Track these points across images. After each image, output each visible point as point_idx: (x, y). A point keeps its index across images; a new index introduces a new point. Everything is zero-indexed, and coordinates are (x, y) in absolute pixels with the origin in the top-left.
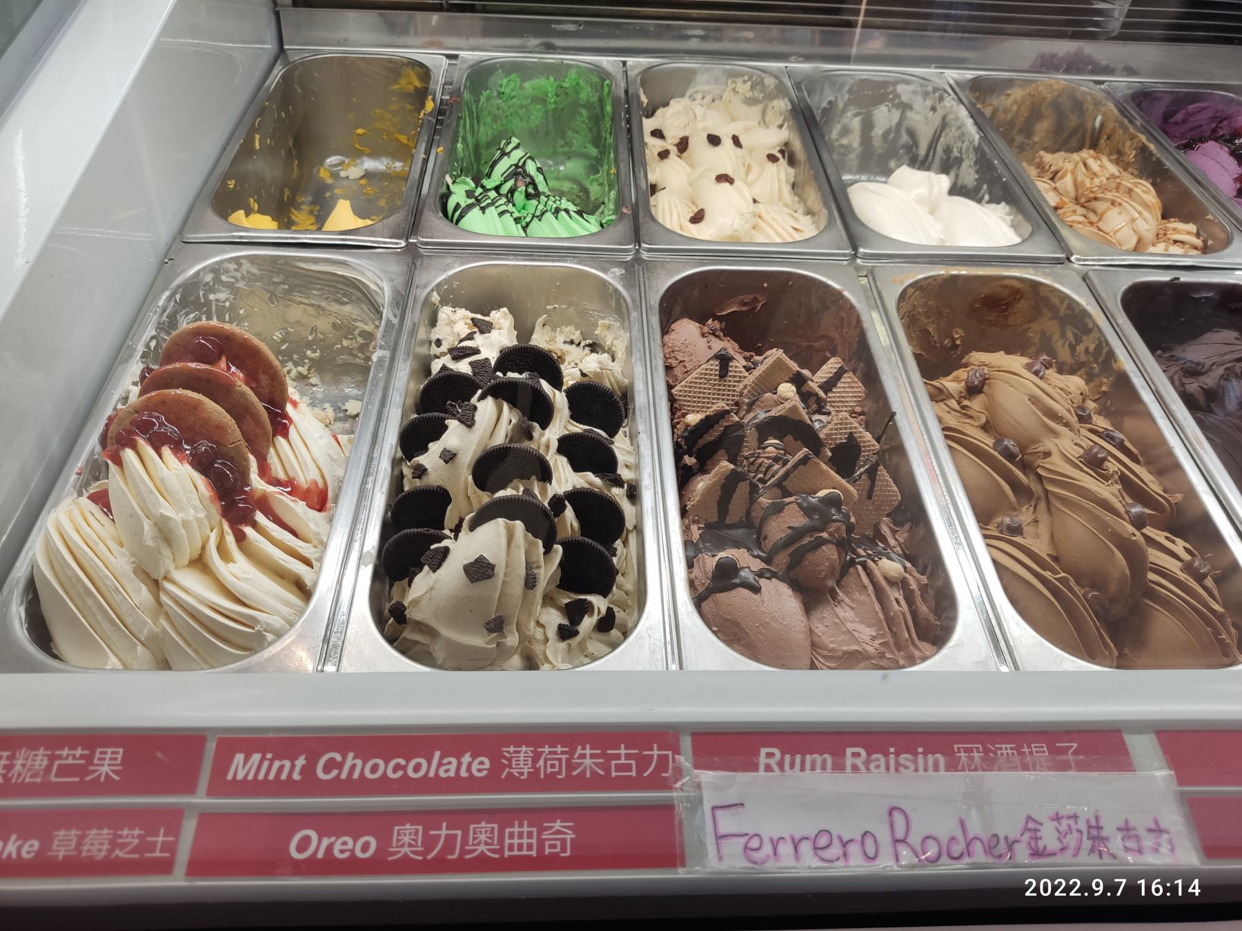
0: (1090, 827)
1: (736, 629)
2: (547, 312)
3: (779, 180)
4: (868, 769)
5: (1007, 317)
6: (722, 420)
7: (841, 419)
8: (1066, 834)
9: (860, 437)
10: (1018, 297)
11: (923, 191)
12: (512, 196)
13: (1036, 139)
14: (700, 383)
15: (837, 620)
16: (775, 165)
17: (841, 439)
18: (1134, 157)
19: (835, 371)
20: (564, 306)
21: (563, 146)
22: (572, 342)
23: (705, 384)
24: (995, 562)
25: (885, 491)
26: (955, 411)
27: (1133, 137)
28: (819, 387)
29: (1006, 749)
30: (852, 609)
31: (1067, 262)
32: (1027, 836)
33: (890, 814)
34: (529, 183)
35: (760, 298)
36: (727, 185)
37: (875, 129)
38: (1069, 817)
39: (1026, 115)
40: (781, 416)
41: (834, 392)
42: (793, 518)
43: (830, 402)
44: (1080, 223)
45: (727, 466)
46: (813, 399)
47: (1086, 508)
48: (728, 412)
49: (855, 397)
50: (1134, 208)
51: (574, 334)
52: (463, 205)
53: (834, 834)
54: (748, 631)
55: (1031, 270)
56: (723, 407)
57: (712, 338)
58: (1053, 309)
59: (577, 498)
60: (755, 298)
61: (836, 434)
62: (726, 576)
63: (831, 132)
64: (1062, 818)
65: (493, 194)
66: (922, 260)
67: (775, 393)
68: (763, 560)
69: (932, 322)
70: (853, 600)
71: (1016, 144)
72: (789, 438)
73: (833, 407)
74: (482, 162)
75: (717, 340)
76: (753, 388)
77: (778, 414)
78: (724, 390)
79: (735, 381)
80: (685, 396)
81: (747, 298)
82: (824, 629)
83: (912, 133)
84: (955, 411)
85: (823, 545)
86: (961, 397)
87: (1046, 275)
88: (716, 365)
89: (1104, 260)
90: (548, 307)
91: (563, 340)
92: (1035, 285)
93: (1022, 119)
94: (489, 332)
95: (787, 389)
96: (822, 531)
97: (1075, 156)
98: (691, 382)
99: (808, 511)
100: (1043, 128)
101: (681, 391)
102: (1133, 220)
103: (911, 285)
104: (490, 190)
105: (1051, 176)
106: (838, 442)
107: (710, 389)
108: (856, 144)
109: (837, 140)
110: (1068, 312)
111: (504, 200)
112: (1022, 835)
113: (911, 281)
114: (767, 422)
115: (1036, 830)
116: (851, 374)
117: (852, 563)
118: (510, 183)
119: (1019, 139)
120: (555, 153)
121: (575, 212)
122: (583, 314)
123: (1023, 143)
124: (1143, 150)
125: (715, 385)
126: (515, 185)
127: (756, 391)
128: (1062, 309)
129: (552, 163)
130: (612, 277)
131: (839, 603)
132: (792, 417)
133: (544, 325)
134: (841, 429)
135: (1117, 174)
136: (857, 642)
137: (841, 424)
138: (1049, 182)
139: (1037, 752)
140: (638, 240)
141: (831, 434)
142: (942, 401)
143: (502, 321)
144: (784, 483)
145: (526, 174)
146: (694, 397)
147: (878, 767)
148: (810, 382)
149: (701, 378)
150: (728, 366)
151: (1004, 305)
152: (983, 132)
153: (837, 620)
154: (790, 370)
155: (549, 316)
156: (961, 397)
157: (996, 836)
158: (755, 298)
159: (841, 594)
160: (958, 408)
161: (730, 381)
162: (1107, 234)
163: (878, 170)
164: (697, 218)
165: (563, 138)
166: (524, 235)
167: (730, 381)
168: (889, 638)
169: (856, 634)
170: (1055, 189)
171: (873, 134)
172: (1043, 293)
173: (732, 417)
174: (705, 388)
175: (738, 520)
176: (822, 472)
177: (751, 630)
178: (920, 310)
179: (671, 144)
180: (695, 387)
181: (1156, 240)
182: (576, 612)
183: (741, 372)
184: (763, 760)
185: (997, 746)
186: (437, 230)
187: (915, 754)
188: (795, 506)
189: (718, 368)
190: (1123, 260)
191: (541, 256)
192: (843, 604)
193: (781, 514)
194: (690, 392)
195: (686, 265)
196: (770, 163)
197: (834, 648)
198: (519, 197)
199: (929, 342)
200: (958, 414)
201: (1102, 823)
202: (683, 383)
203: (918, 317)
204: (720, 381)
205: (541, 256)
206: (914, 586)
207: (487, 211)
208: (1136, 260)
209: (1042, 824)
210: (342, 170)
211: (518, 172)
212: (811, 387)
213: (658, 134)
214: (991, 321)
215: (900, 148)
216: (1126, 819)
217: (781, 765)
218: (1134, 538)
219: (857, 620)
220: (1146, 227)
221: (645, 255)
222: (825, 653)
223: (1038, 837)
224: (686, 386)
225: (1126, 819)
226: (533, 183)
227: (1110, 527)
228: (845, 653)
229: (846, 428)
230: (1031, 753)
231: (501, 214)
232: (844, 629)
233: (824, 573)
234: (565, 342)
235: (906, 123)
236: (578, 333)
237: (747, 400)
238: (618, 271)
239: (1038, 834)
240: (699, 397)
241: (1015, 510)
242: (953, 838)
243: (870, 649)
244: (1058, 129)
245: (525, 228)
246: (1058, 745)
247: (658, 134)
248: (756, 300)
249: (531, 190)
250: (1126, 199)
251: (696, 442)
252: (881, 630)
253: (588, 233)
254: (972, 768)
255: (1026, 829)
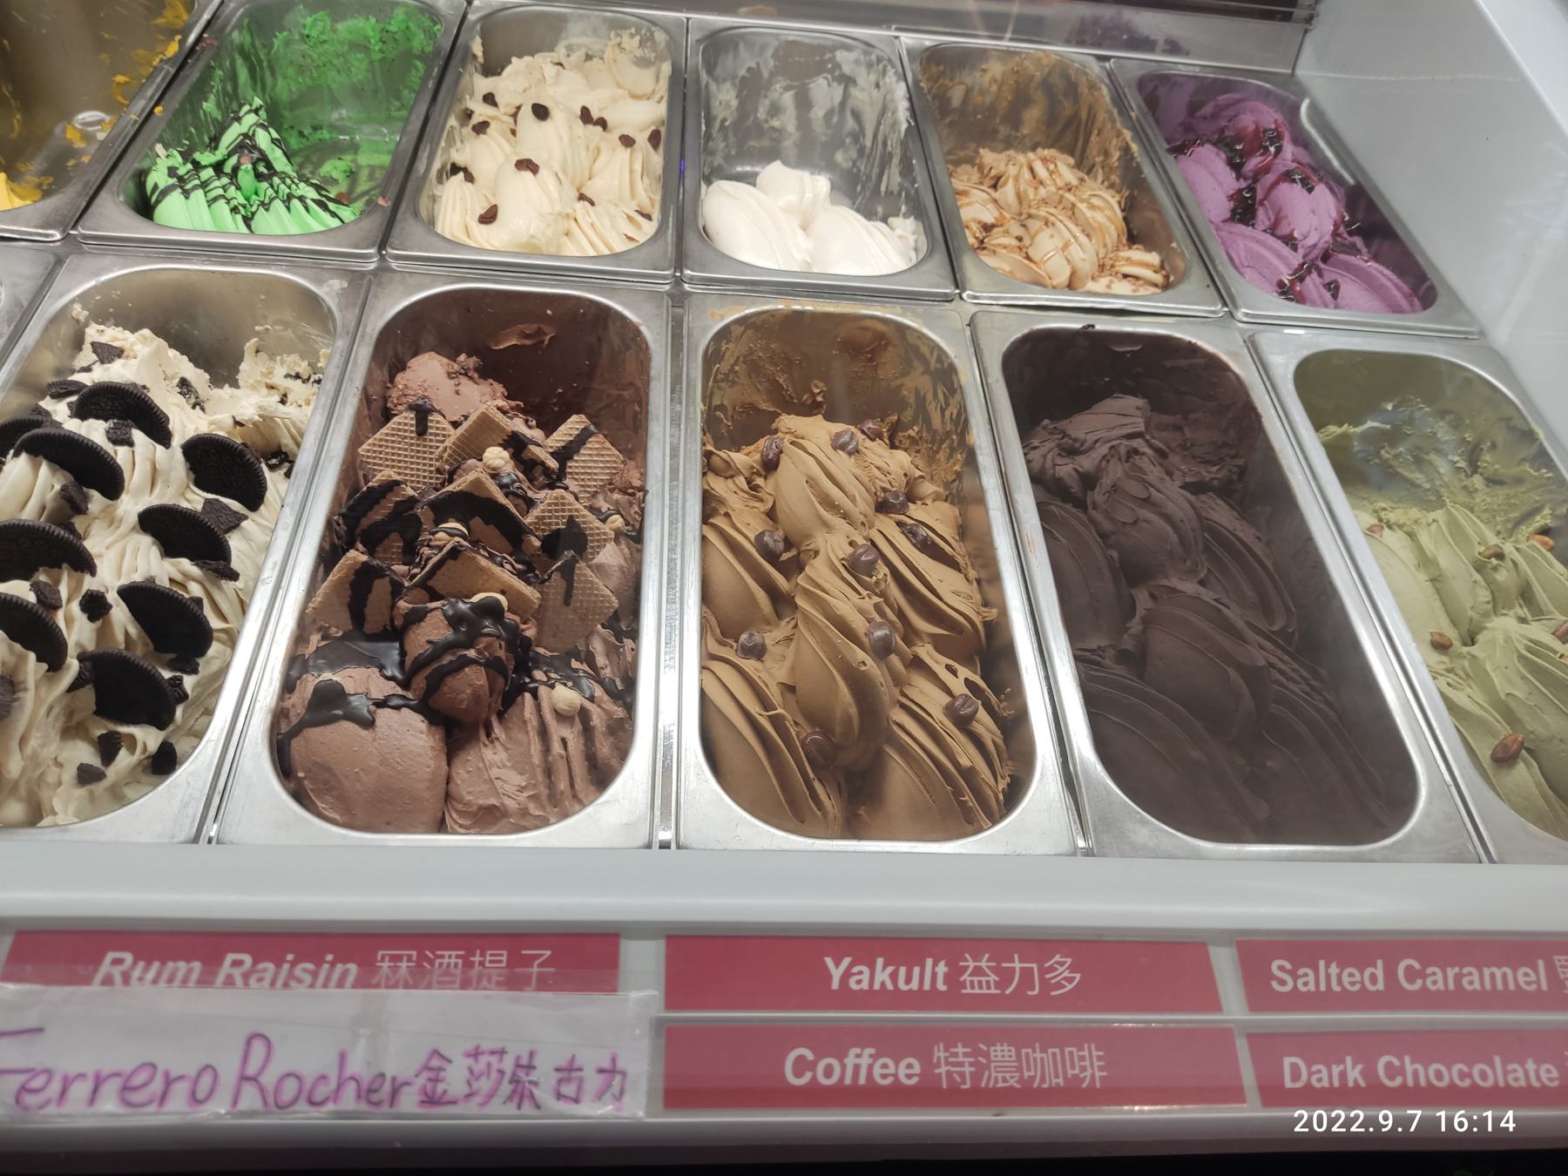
0: (518, 1066)
1: (327, 776)
2: (257, 334)
3: (631, 171)
4: (246, 984)
5: (875, 368)
6: (390, 494)
7: (556, 498)
8: (481, 1075)
9: (584, 523)
10: (883, 343)
11: (792, 198)
12: (236, 176)
13: (1025, 131)
14: (393, 442)
15: (481, 765)
16: (629, 150)
17: (557, 524)
18: (1119, 159)
19: (577, 432)
20: (278, 328)
21: (399, 109)
22: (297, 376)
23: (400, 443)
24: (703, 694)
25: (589, 595)
26: (743, 491)
27: (1119, 134)
28: (552, 454)
29: (450, 957)
30: (507, 749)
31: (957, 299)
32: (426, 1075)
33: (249, 1042)
34: (258, 160)
35: (545, 328)
36: (528, 174)
37: (815, 109)
38: (493, 1053)
39: (1009, 98)
40: (461, 491)
41: (577, 461)
42: (433, 630)
43: (570, 473)
44: (1005, 247)
45: (354, 558)
46: (539, 469)
47: (819, 627)
48: (397, 483)
49: (608, 468)
50: (1069, 230)
51: (300, 366)
52: (162, 186)
53: (161, 1069)
54: (342, 778)
55: (898, 309)
56: (390, 476)
57: (464, 380)
58: (924, 360)
59: (140, 597)
60: (540, 329)
61: (550, 517)
62: (329, 703)
63: (756, 110)
64: (483, 1053)
65: (208, 173)
66: (766, 288)
67: (481, 460)
68: (399, 683)
69: (782, 371)
70: (509, 737)
71: (1000, 136)
72: (476, 522)
73: (576, 479)
74: (286, 126)
75: (470, 383)
76: (454, 451)
77: (458, 489)
78: (425, 452)
79: (438, 441)
80: (375, 458)
81: (530, 328)
82: (466, 776)
83: (857, 116)
84: (743, 491)
85: (466, 666)
86: (753, 473)
87: (916, 315)
88: (412, 419)
89: (1005, 299)
90: (257, 328)
91: (285, 372)
92: (901, 328)
93: (1004, 103)
94: (110, 362)
95: (497, 456)
96: (468, 648)
97: (1021, 158)
98: (381, 440)
99: (455, 621)
100: (1033, 116)
101: (368, 451)
102: (1066, 246)
103: (738, 322)
104: (205, 167)
105: (992, 182)
106: (554, 527)
107: (406, 450)
108: (791, 127)
109: (766, 121)
110: (938, 366)
111: (225, 180)
112: (417, 1076)
113: (736, 316)
114: (444, 499)
115: (440, 1069)
116: (601, 438)
117: (522, 688)
118: (233, 161)
119: (1004, 130)
120: (389, 118)
121: (313, 200)
122: (304, 339)
123: (1010, 136)
124: (1126, 150)
125: (412, 444)
126: (239, 161)
127: (459, 455)
128: (933, 364)
129: (386, 131)
130: (330, 291)
131: (492, 742)
132: (476, 493)
133: (257, 351)
134: (557, 511)
135: (1075, 182)
136: (497, 794)
137: (556, 504)
138: (990, 191)
139: (491, 962)
140: (382, 246)
141: (544, 517)
142: (732, 477)
143: (138, 347)
144: (430, 583)
145: (255, 147)
146: (387, 460)
147: (260, 980)
148: (533, 448)
149: (393, 435)
150: (426, 420)
151: (868, 353)
152: (916, 121)
153: (481, 765)
154: (502, 430)
155: (261, 339)
156: (753, 473)
157: (382, 1075)
158: (540, 329)
159: (498, 730)
160: (746, 487)
161: (431, 440)
162: (1035, 263)
163: (823, 164)
164: (489, 217)
165: (398, 98)
166: (246, 231)
167: (431, 440)
168: (544, 791)
169: (498, 784)
170: (995, 201)
171: (812, 115)
172: (912, 339)
173: (404, 490)
174: (400, 449)
175: (381, 628)
176: (482, 569)
177: (346, 777)
178: (761, 354)
179: (505, 114)
180: (387, 447)
181: (1097, 274)
182: (108, 748)
183: (444, 429)
184: (106, 967)
185: (438, 953)
186: (114, 216)
187: (279, 965)
188: (438, 613)
189: (413, 422)
190: (1030, 299)
191: (243, 258)
192: (497, 743)
193: (423, 624)
194: (381, 452)
195: (436, 279)
196: (623, 148)
197: (470, 801)
198: (246, 177)
199: (783, 397)
200: (746, 496)
201: (537, 1062)
202: (370, 441)
203: (762, 363)
204: (418, 439)
205: (243, 258)
206: (597, 720)
207: (193, 195)
208: (1047, 300)
209: (450, 1061)
210: (100, 130)
211: (246, 144)
212: (533, 454)
213: (489, 99)
214: (856, 373)
215: (847, 136)
216: (574, 1056)
217: (126, 978)
218: (863, 668)
219: (508, 764)
220: (1082, 255)
221: (394, 264)
222: (460, 807)
223: (440, 1078)
224: (374, 445)
225: (574, 1056)
226: (264, 158)
227: (840, 652)
228: (481, 808)
229: (563, 510)
230: (482, 964)
231: (211, 202)
232: (486, 777)
233: (465, 703)
234: (288, 376)
235: (851, 103)
236: (305, 364)
237: (447, 467)
238: (338, 284)
239: (442, 1074)
240: (393, 461)
241: (769, 623)
242: (323, 1077)
243: (511, 804)
244: (1051, 118)
245: (247, 221)
246: (524, 952)
247: (489, 99)
248: (540, 332)
249: (262, 169)
250: (1061, 218)
251: (357, 521)
252: (532, 779)
253: (324, 229)
254: (391, 983)
255: (427, 1068)
